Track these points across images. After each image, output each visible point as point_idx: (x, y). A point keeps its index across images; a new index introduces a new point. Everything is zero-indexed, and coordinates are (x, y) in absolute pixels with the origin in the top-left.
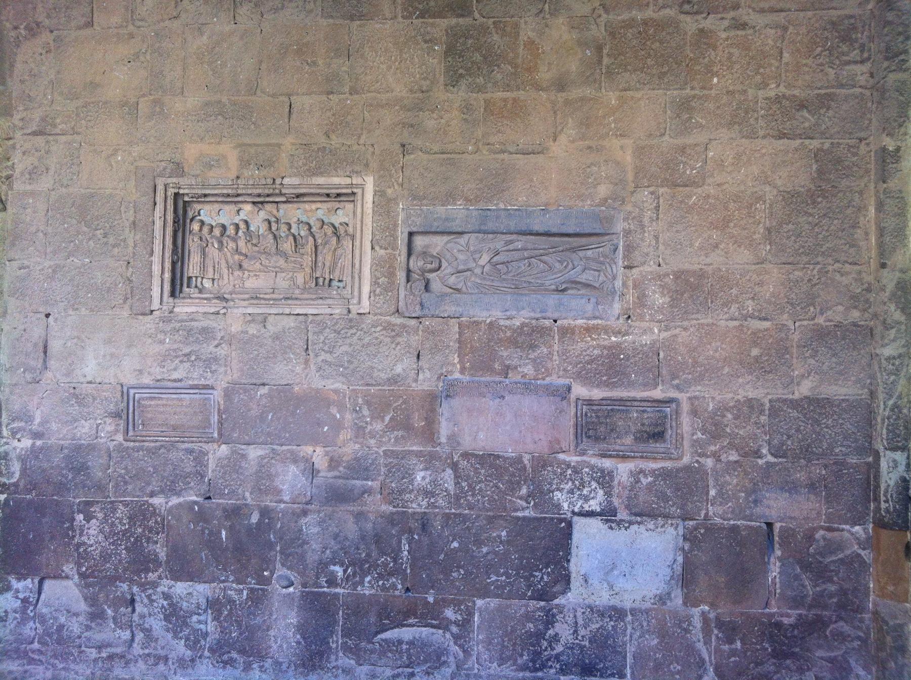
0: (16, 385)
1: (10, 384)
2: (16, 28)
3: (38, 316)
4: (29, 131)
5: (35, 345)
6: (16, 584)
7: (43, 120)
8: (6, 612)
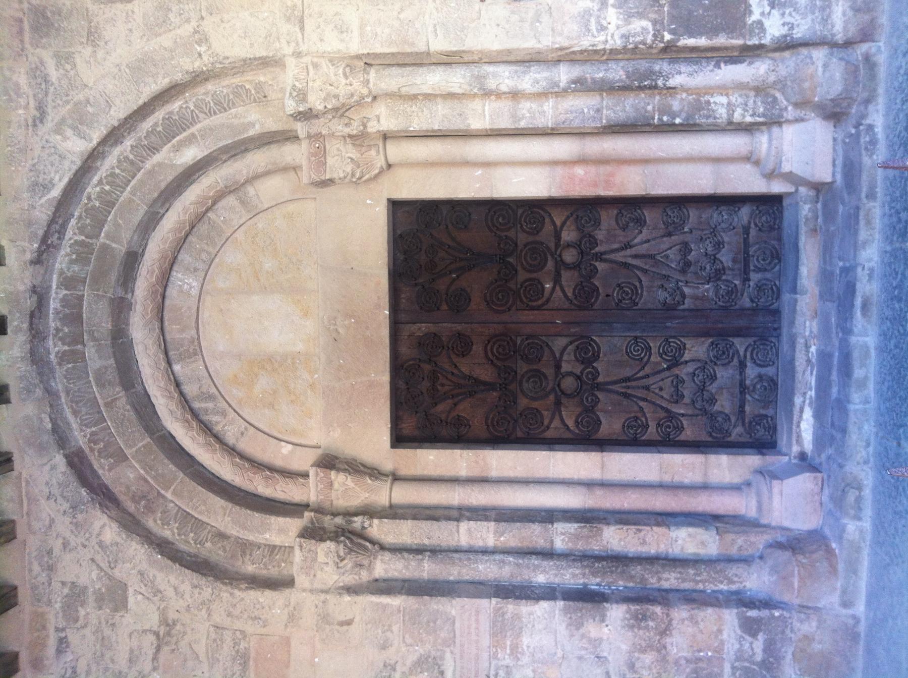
0: (553, 30)
1: (553, 36)
2: (200, 55)
3: (483, 12)
4: (300, 35)
5: (513, 12)
6: (755, 17)
7: (288, 20)
8: (784, 24)
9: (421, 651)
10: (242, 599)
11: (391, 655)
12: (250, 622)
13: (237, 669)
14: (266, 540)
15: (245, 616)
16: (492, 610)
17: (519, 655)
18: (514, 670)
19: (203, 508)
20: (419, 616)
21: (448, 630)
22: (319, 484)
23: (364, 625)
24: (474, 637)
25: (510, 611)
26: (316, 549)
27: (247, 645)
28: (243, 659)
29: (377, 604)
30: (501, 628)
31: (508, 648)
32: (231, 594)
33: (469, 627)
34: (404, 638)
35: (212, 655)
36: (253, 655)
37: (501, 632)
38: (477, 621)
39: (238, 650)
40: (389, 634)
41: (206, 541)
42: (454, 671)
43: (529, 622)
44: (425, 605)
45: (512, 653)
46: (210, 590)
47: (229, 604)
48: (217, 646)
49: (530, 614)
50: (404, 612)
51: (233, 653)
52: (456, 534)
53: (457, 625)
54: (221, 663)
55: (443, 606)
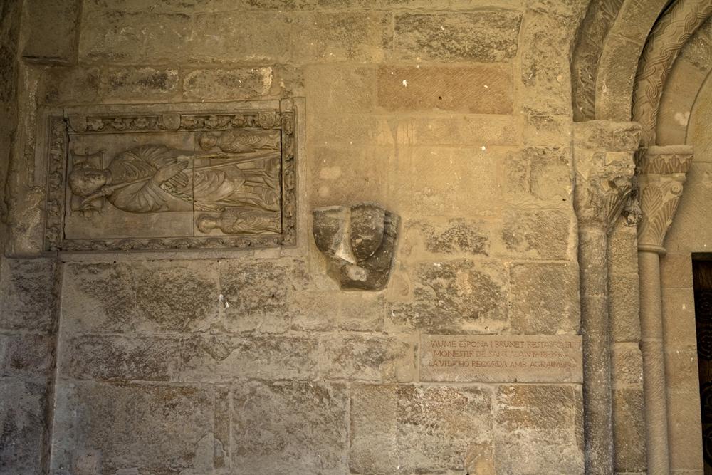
9: (504, 289)
10: (559, 54)
11: (496, 247)
12: (529, 63)
13: (467, 45)
14: (600, 89)
15: (536, 57)
16: (567, 385)
17: (506, 423)
18: (484, 416)
19: (636, 11)
20: (552, 285)
21: (536, 324)
22: (670, 157)
23: (537, 212)
24: (529, 360)
25: (568, 410)
26: (625, 150)
27: (498, 58)
28: (480, 52)
29: (566, 230)
30: (543, 398)
31: (516, 408)
32: (564, 40)
33: (543, 353)
34: (522, 265)
35: (483, 14)
36: (487, 65)
37: (537, 398)
38: (552, 365)
39: (491, 47)
40: (525, 244)
41: (604, 13)
42: (478, 333)
43: (553, 437)
44: (568, 293)
45: (513, 412)
46: (569, 13)
47: (551, 37)
48: (495, 21)
49: (566, 440)
50: (558, 265)
51: (487, 41)
52: (624, 339)
53: (544, 337)
54: (472, 25)
55: (569, 317)
